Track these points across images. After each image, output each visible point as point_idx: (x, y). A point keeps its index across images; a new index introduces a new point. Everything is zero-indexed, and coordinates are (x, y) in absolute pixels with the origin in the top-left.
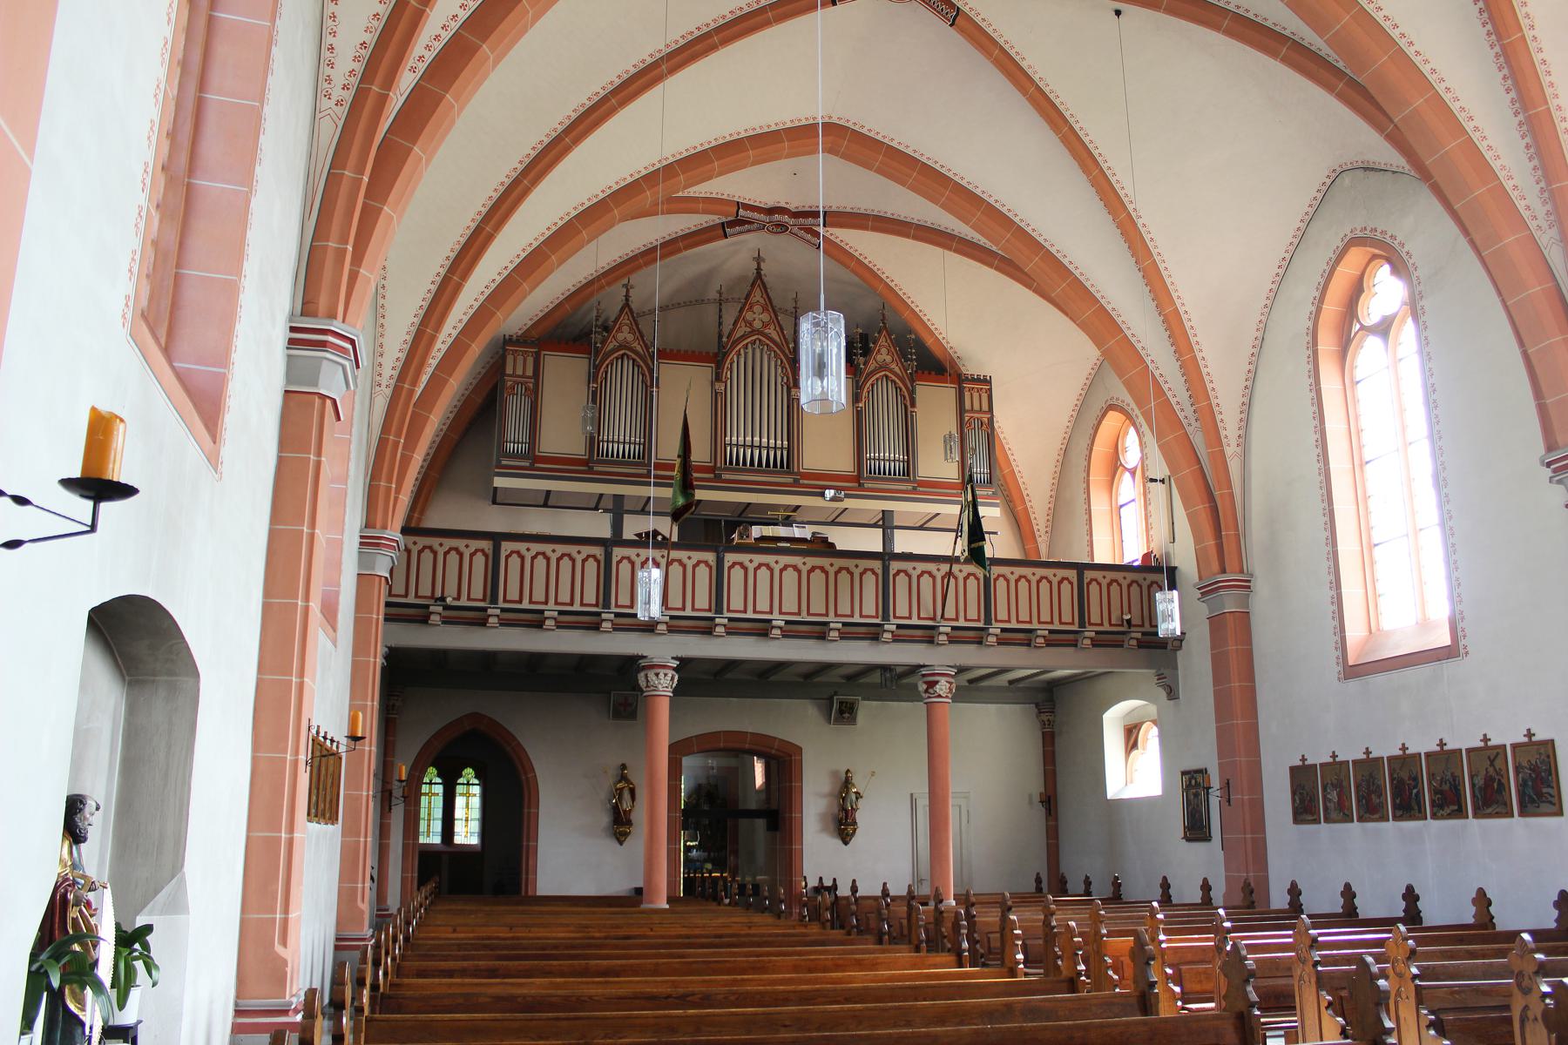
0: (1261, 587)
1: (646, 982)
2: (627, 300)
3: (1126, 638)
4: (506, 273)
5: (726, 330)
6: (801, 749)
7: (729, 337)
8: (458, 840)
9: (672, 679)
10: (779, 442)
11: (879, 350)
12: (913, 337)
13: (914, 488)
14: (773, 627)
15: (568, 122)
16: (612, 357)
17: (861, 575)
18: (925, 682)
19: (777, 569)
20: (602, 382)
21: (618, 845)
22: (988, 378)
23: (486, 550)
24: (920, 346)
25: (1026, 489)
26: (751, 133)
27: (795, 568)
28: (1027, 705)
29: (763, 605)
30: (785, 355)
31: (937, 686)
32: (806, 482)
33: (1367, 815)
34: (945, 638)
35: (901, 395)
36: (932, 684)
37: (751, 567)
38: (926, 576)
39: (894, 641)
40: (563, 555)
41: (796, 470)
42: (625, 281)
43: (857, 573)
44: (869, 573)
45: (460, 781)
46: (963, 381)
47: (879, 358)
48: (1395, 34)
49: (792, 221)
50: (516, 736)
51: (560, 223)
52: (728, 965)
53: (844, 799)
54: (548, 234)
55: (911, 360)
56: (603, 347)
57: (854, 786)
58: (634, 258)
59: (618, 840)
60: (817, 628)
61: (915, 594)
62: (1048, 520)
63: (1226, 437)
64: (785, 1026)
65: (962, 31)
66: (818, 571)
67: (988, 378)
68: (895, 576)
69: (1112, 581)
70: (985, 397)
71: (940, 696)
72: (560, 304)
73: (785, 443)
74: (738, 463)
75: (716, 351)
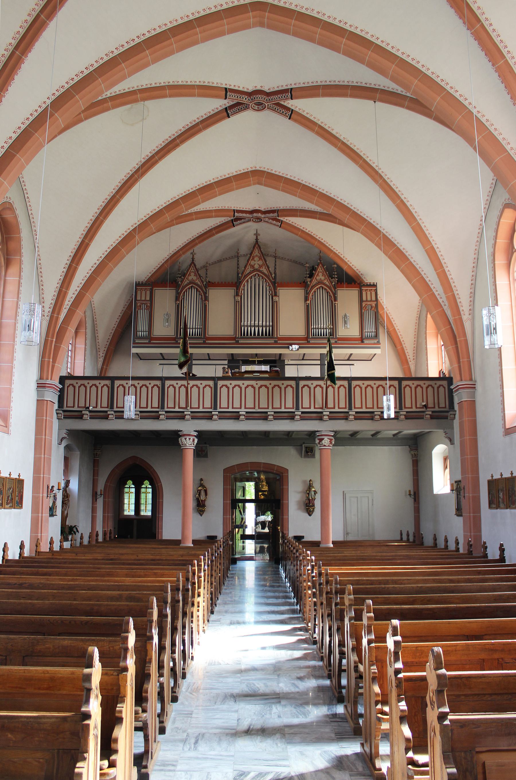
0: (479, 387)
1: (36, 578)
2: (193, 260)
3: (424, 414)
4: (101, 259)
5: (240, 271)
6: (287, 471)
8: (142, 513)
9: (194, 440)
10: (268, 323)
11: (318, 274)
13: (336, 342)
14: (240, 415)
15: (117, 188)
16: (186, 288)
17: (285, 388)
18: (319, 439)
19: (243, 387)
20: (182, 300)
21: (200, 516)
22: (375, 284)
23: (108, 385)
24: (339, 268)
25: (402, 338)
26: (216, 180)
27: (252, 386)
28: (404, 447)
29: (237, 404)
30: (270, 280)
31: (323, 441)
32: (281, 342)
33: (512, 506)
34: (327, 417)
35: (330, 296)
37: (231, 387)
38: (318, 387)
39: (301, 419)
40: (143, 385)
41: (275, 336)
42: (191, 251)
43: (283, 387)
44: (289, 387)
45: (143, 486)
46: (362, 286)
47: (318, 278)
48: (466, 103)
49: (263, 216)
50: (153, 467)
51: (126, 234)
52: (97, 573)
53: (308, 494)
54: (120, 239)
55: (334, 278)
56: (182, 284)
57: (313, 487)
58: (194, 240)
59: (200, 513)
60: (263, 415)
61: (312, 396)
62: (414, 353)
63: (463, 310)
64: (23, 598)
65: (296, 121)
66: (263, 387)
68: (302, 388)
69: (418, 386)
70: (373, 293)
71: (325, 446)
72: (163, 265)
73: (271, 323)
75: (236, 281)
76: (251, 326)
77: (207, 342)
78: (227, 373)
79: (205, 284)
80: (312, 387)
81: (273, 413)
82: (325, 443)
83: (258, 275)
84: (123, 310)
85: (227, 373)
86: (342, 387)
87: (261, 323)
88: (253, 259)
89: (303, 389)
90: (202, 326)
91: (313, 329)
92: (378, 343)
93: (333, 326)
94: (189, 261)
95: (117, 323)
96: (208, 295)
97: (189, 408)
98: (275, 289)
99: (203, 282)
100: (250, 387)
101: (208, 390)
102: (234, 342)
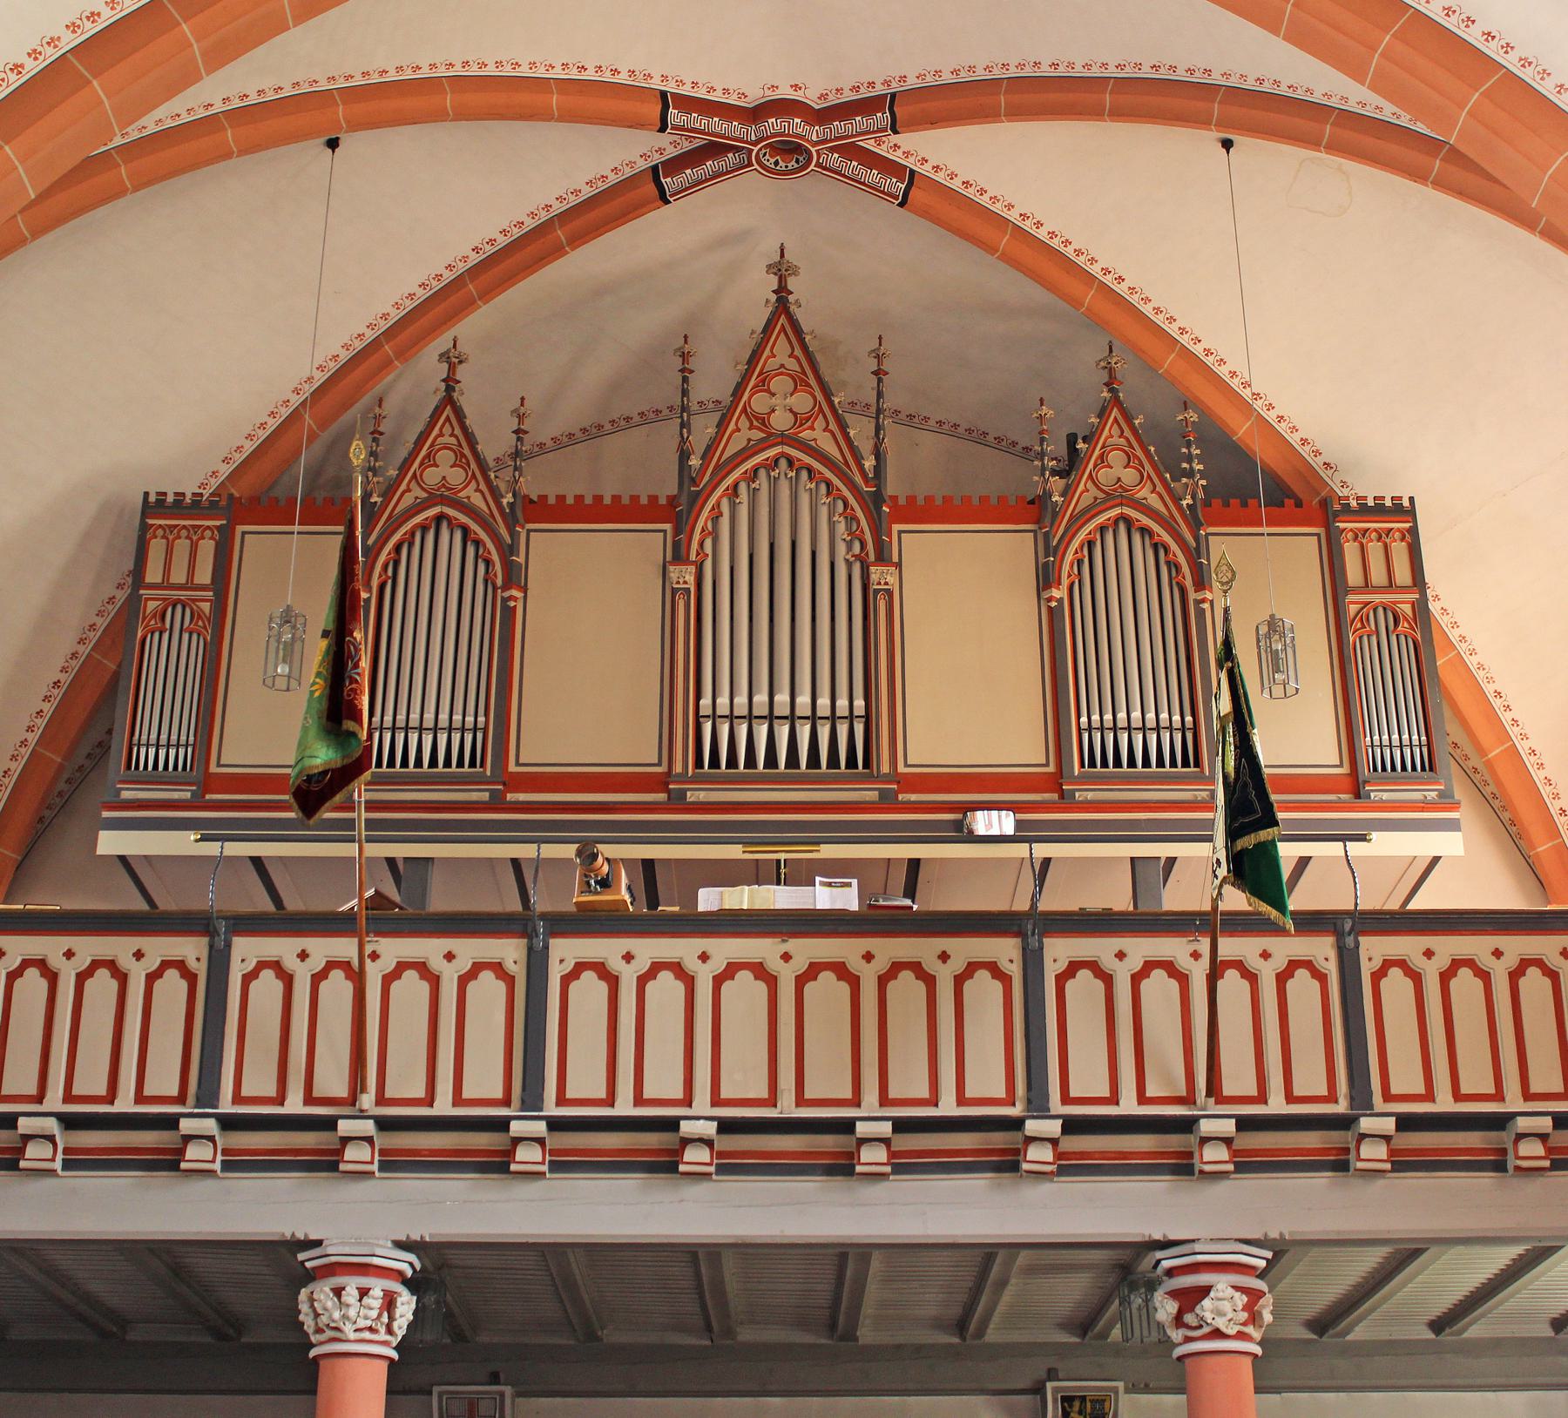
2: (449, 389)
7: (707, 455)
9: (389, 1302)
10: (842, 703)
11: (1102, 457)
12: (1193, 417)
14: (686, 1142)
17: (959, 981)
18: (1174, 1294)
22: (1406, 503)
25: (1556, 796)
27: (760, 971)
29: (664, 1080)
31: (1206, 1303)
32: (914, 797)
35: (1168, 563)
36: (1191, 1298)
37: (628, 977)
38: (1159, 975)
39: (1063, 1171)
41: (885, 769)
42: (442, 343)
43: (945, 977)
44: (983, 975)
46: (1336, 514)
49: (815, 133)
51: (32, 67)
55: (1190, 474)
60: (828, 1142)
66: (827, 977)
67: (1406, 503)
68: (1061, 979)
70: (1400, 551)
71: (1217, 1334)
73: (859, 703)
74: (732, 762)
75: (673, 489)
76: (750, 718)
77: (510, 797)
78: (605, 883)
79: (511, 505)
80: (1122, 975)
81: (886, 1128)
82: (1221, 1314)
83: (791, 462)
84: (74, 655)
85: (605, 883)
86: (1302, 974)
87: (804, 699)
88: (763, 385)
89: (1070, 985)
90: (486, 714)
91: (1090, 729)
93: (1194, 714)
95: (41, 723)
96: (521, 559)
97: (367, 1101)
99: (496, 494)
100: (745, 976)
101: (488, 990)
102: (662, 797)
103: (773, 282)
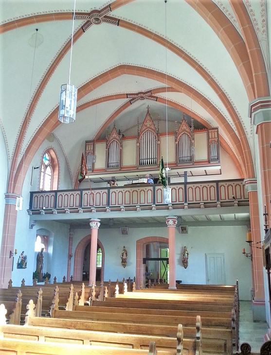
4: (40, 126)
24: (196, 122)
27: (129, 191)
36: (168, 221)
47: (183, 128)
65: (122, 26)
70: (216, 133)
92: (219, 162)
94: (112, 127)
98: (158, 136)
103: (147, 109)
